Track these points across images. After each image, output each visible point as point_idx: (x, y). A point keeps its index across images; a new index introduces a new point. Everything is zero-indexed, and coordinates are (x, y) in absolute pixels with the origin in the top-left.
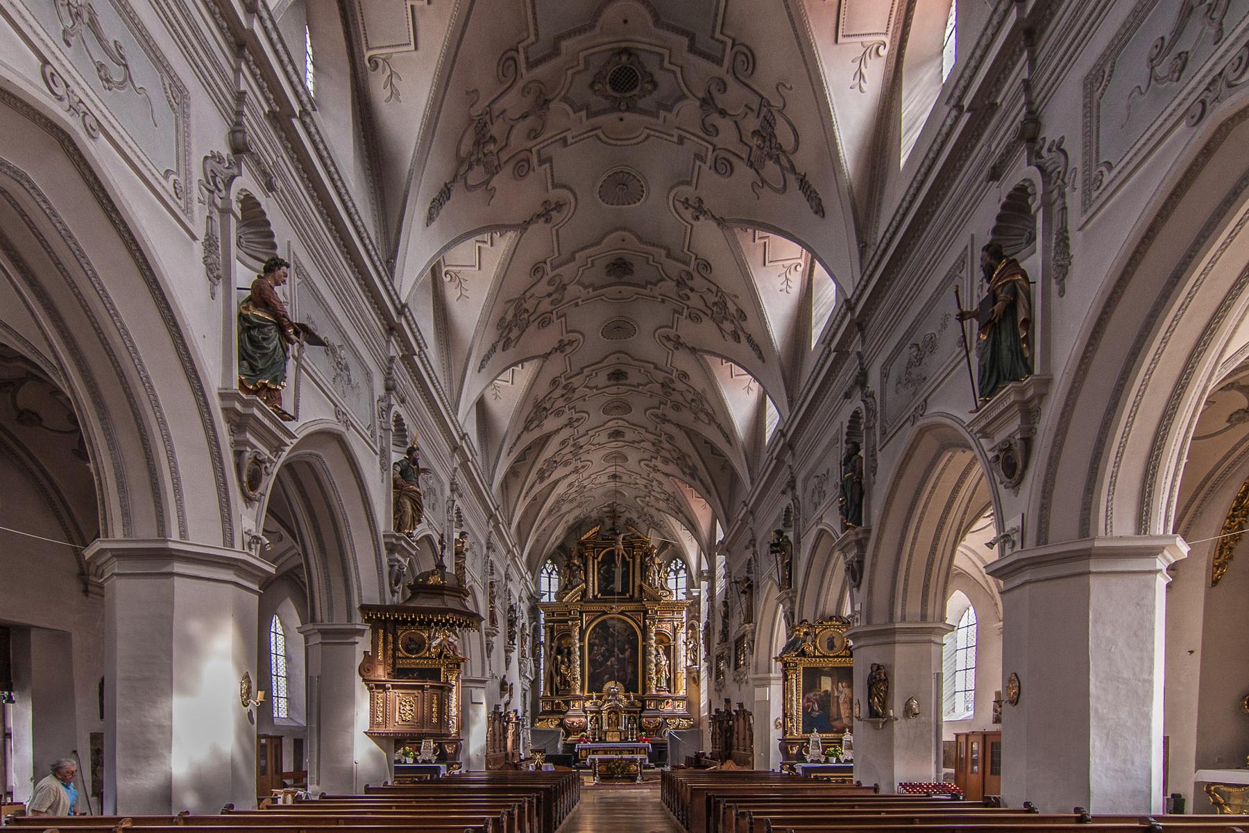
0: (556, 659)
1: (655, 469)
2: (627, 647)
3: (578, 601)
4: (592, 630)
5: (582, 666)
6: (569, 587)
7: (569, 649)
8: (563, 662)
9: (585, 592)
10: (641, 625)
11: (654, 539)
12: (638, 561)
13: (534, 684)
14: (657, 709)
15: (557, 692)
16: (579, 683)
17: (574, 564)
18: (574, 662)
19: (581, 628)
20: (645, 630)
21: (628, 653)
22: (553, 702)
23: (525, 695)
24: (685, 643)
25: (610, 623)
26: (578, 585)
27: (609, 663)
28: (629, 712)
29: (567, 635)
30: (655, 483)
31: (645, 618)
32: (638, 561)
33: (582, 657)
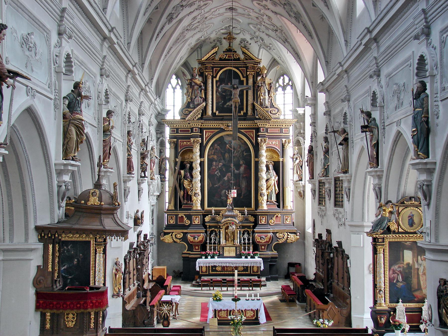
0: (179, 173)
1: (265, 7)
2: (241, 162)
5: (202, 181)
6: (191, 106)
7: (191, 163)
8: (185, 177)
9: (205, 110)
10: (254, 142)
11: (264, 63)
13: (160, 197)
14: (268, 224)
15: (181, 206)
16: (200, 198)
17: (196, 84)
18: (195, 178)
19: (201, 145)
20: (257, 147)
21: (242, 169)
22: (177, 216)
23: (153, 211)
24: (293, 158)
25: (227, 139)
26: (198, 105)
27: (226, 178)
28: (243, 227)
29: (190, 150)
30: (265, 17)
31: (257, 136)
32: (251, 81)
33: (202, 173)
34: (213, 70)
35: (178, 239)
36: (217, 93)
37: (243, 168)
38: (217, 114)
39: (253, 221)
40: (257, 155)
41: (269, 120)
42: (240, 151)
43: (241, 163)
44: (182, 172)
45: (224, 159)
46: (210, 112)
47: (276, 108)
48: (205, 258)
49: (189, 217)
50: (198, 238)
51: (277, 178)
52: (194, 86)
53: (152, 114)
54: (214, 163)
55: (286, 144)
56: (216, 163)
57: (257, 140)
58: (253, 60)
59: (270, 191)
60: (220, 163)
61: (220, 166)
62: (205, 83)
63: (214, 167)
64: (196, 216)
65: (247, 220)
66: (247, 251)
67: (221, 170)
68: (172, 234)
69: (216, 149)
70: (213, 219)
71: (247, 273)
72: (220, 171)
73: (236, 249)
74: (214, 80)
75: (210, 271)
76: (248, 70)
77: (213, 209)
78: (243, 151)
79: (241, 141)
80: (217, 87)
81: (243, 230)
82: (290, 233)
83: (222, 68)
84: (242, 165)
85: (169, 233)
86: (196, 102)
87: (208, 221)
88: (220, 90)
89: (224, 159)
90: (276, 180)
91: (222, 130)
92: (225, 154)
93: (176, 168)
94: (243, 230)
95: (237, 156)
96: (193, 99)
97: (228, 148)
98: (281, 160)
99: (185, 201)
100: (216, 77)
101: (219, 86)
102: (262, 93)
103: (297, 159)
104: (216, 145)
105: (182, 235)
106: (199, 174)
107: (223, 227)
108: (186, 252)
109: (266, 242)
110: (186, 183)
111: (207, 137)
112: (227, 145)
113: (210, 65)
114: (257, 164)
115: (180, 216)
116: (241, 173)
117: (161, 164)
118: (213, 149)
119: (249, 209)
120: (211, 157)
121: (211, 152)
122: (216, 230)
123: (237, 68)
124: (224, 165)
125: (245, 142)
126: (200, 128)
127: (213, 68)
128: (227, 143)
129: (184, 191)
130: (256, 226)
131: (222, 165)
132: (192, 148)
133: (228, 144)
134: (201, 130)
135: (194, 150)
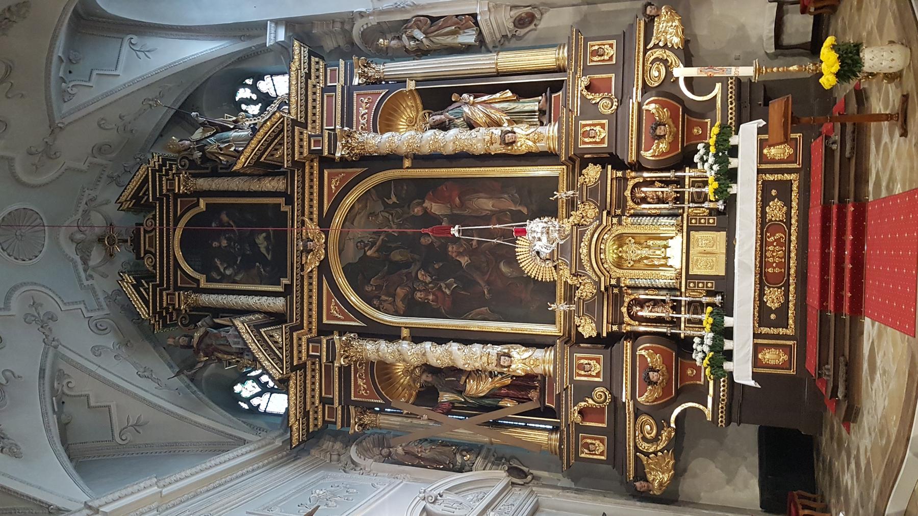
5: (466, 338)
10: (359, 171)
12: (203, 183)
17: (201, 339)
22: (579, 428)
25: (352, 255)
27: (464, 261)
32: (203, 183)
33: (440, 337)
35: (659, 434)
36: (238, 278)
37: (433, 204)
39: (599, 167)
40: (392, 159)
41: (283, 122)
42: (386, 215)
43: (420, 214)
44: (446, 397)
45: (407, 265)
46: (278, 304)
48: (730, 337)
49: (583, 391)
52: (208, 346)
54: (418, 295)
56: (420, 291)
57: (344, 163)
60: (420, 276)
61: (428, 279)
63: (431, 297)
65: (595, 193)
66: (706, 190)
67: (439, 276)
68: (642, 452)
69: (379, 287)
70: (591, 308)
71: (795, 187)
72: (444, 279)
74: (203, 284)
75: (782, 331)
77: (560, 307)
78: (386, 205)
79: (358, 213)
80: (223, 278)
81: (630, 203)
82: (647, 41)
83: (177, 265)
84: (425, 209)
85: (637, 458)
87: (594, 325)
88: (228, 272)
89: (407, 265)
91: (324, 268)
92: (391, 262)
94: (630, 203)
97: (377, 251)
98: (411, 85)
99: (534, 394)
100: (197, 281)
101: (219, 273)
102: (221, 149)
103: (413, 38)
104: (368, 288)
105: (644, 418)
106: (440, 350)
107: (613, 275)
108: (708, 411)
109: (674, 117)
111: (342, 312)
112: (369, 253)
113: (165, 298)
115: (577, 417)
116: (448, 212)
119: (563, 184)
120: (400, 305)
121: (386, 305)
122: (627, 300)
123: (177, 221)
124: (424, 267)
125: (359, 200)
131: (427, 271)
132: (372, 363)
133: (365, 252)
134: (325, 330)
135: (373, 357)
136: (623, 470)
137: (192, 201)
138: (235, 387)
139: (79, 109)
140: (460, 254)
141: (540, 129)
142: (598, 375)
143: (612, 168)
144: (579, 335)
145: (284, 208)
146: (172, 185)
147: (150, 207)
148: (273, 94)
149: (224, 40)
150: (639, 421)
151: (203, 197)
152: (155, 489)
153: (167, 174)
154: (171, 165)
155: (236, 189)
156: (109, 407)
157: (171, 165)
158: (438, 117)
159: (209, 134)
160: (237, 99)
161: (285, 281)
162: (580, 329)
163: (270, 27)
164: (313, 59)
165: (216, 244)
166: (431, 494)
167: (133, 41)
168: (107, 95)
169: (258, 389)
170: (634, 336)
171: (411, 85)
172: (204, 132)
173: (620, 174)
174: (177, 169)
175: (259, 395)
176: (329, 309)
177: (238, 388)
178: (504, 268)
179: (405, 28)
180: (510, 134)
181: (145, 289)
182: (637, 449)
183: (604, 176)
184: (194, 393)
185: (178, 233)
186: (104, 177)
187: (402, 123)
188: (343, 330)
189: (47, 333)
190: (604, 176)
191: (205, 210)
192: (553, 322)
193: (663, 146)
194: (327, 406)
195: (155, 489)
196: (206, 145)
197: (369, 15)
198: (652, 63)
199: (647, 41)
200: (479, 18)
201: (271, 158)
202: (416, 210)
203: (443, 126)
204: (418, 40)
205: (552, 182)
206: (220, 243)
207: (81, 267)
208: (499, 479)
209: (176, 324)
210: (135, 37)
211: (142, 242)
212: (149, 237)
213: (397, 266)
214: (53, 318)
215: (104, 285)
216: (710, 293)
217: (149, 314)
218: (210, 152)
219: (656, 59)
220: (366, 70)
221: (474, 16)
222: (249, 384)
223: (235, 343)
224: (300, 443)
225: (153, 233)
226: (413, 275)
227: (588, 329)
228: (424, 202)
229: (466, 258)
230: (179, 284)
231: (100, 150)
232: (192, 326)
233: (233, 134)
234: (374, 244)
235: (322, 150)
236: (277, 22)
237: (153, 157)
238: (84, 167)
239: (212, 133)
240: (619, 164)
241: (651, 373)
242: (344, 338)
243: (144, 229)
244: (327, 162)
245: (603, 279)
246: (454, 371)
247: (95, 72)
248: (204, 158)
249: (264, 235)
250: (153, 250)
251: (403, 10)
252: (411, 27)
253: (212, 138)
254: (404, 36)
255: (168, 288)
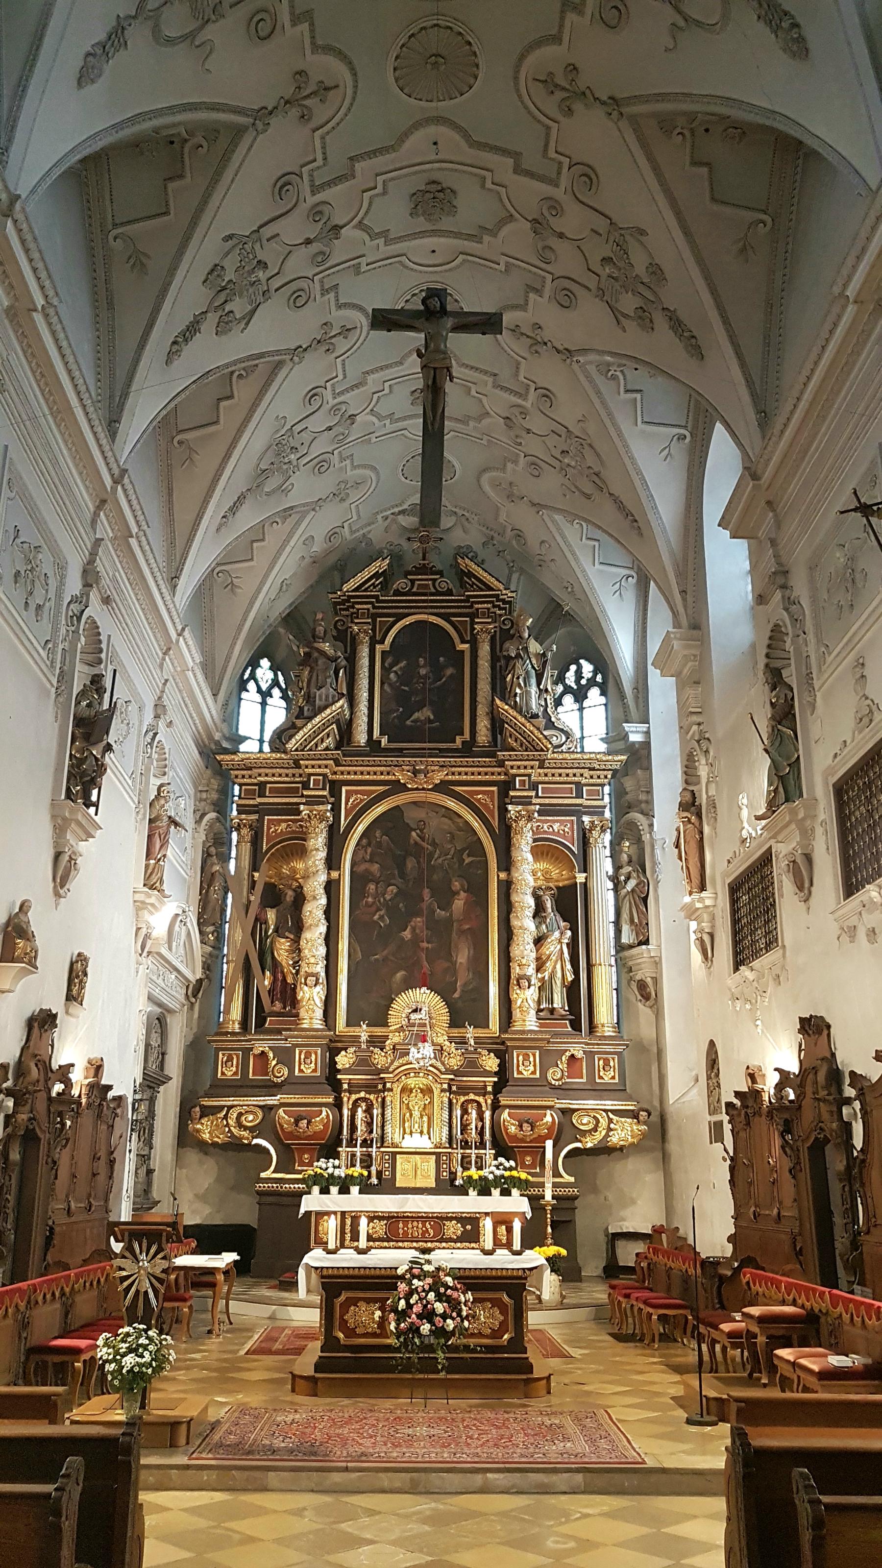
0: (260, 920)
3: (327, 749)
4: (364, 835)
5: (330, 939)
9: (346, 730)
10: (495, 824)
12: (485, 649)
17: (322, 653)
19: (332, 830)
22: (247, 1051)
25: (412, 816)
27: (407, 934)
32: (485, 649)
33: (331, 913)
34: (374, 621)
35: (246, 1128)
36: (386, 687)
37: (462, 902)
38: (383, 744)
39: (497, 1069)
40: (506, 862)
41: (542, 750)
42: (452, 852)
43: (453, 888)
44: (271, 915)
45: (403, 875)
46: (361, 737)
47: (562, 730)
49: (286, 1057)
50: (309, 1123)
51: (569, 933)
52: (316, 660)
53: (167, 681)
54: (372, 887)
55: (595, 834)
56: (377, 888)
58: (492, 589)
59: (547, 975)
60: (391, 888)
61: (388, 897)
62: (352, 660)
64: (305, 1050)
65: (472, 1066)
66: (473, 1169)
67: (391, 909)
69: (379, 845)
70: (363, 1063)
73: (438, 1162)
76: (476, 620)
77: (363, 1032)
79: (454, 822)
80: (385, 670)
84: (458, 893)
85: (221, 1108)
86: (320, 699)
87: (347, 1066)
88: (392, 676)
89: (403, 875)
90: (566, 941)
91: (398, 787)
93: (252, 898)
95: (442, 865)
96: (312, 696)
97: (416, 843)
100: (382, 642)
101: (392, 666)
102: (518, 678)
103: (628, 878)
105: (260, 1115)
106: (320, 914)
107: (395, 1085)
110: (282, 949)
111: (354, 806)
112: (414, 834)
113: (365, 606)
114: (506, 888)
115: (257, 1051)
117: (207, 892)
118: (369, 844)
119: (481, 1033)
120: (362, 868)
122: (372, 1097)
123: (446, 617)
124: (400, 893)
126: (333, 783)
127: (374, 617)
128: (413, 826)
129: (274, 974)
130: (506, 1086)
131: (396, 894)
133: (415, 830)
134: (335, 787)
135: (311, 843)
136: (208, 1095)
137: (466, 633)
138: (266, 659)
139: (559, 529)
140: (414, 929)
141: (533, 1013)
142: (301, 1071)
143: (495, 1082)
144: (337, 1051)
145: (459, 740)
146: (483, 614)
147: (463, 585)
148: (586, 704)
149: (634, 671)
150: (257, 1109)
151: (471, 646)
152: (191, 664)
153: (494, 606)
154: (505, 609)
155: (479, 687)
156: (252, 559)
157: (505, 609)
158: (549, 905)
159: (534, 662)
160: (582, 661)
161: (384, 741)
162: (343, 1053)
163: (643, 727)
164: (610, 772)
165: (421, 661)
166: (188, 919)
167: (630, 579)
168: (574, 554)
169: (264, 687)
170: (338, 1105)
171: (581, 878)
172: (537, 655)
173: (489, 1089)
174: (501, 615)
175: (259, 690)
176: (357, 792)
177: (265, 663)
178: (399, 975)
179: (638, 871)
180: (527, 984)
181: (373, 584)
182: (230, 1107)
183: (487, 1074)
184: (264, 633)
185: (433, 619)
186: (492, 533)
187: (542, 865)
188: (336, 809)
189: (329, 499)
190: (487, 1074)
191: (458, 649)
192: (348, 1024)
193: (513, 1129)
194: (257, 787)
195: (191, 664)
196: (522, 659)
197: (650, 833)
198: (594, 1117)
199: (613, 1112)
200: (644, 947)
201: (508, 734)
202: (457, 883)
203: (539, 912)
204: (626, 883)
205: (484, 1023)
206: (422, 667)
207: (396, 510)
208: (194, 972)
209: (336, 614)
210: (635, 580)
211: (424, 577)
212: (428, 585)
213: (401, 866)
214: (343, 500)
215: (378, 534)
216: (379, 1174)
217: (347, 591)
218: (515, 664)
219: (598, 1121)
220: (599, 828)
221: (646, 942)
222: (270, 675)
223: (320, 696)
224: (219, 762)
225: (433, 590)
226: (392, 881)
227: (343, 1060)
228: (465, 892)
229: (409, 936)
230: (378, 619)
231: (519, 535)
232: (335, 633)
233: (534, 690)
234: (423, 839)
235: (515, 789)
236: (648, 733)
237: (512, 592)
238: (501, 520)
239: (536, 666)
240: (498, 1088)
241: (306, 1121)
242: (328, 814)
243: (436, 579)
244: (506, 786)
245: (391, 1075)
246: (298, 928)
247: (596, 544)
248: (509, 658)
249: (432, 717)
250: (415, 590)
251: (654, 871)
252: (638, 877)
253: (530, 666)
254: (631, 868)
255: (374, 607)
